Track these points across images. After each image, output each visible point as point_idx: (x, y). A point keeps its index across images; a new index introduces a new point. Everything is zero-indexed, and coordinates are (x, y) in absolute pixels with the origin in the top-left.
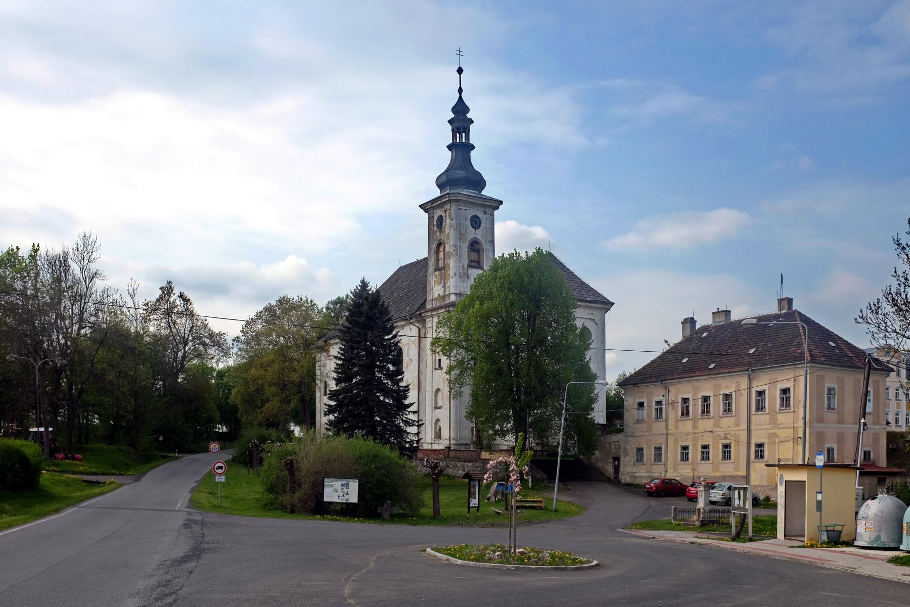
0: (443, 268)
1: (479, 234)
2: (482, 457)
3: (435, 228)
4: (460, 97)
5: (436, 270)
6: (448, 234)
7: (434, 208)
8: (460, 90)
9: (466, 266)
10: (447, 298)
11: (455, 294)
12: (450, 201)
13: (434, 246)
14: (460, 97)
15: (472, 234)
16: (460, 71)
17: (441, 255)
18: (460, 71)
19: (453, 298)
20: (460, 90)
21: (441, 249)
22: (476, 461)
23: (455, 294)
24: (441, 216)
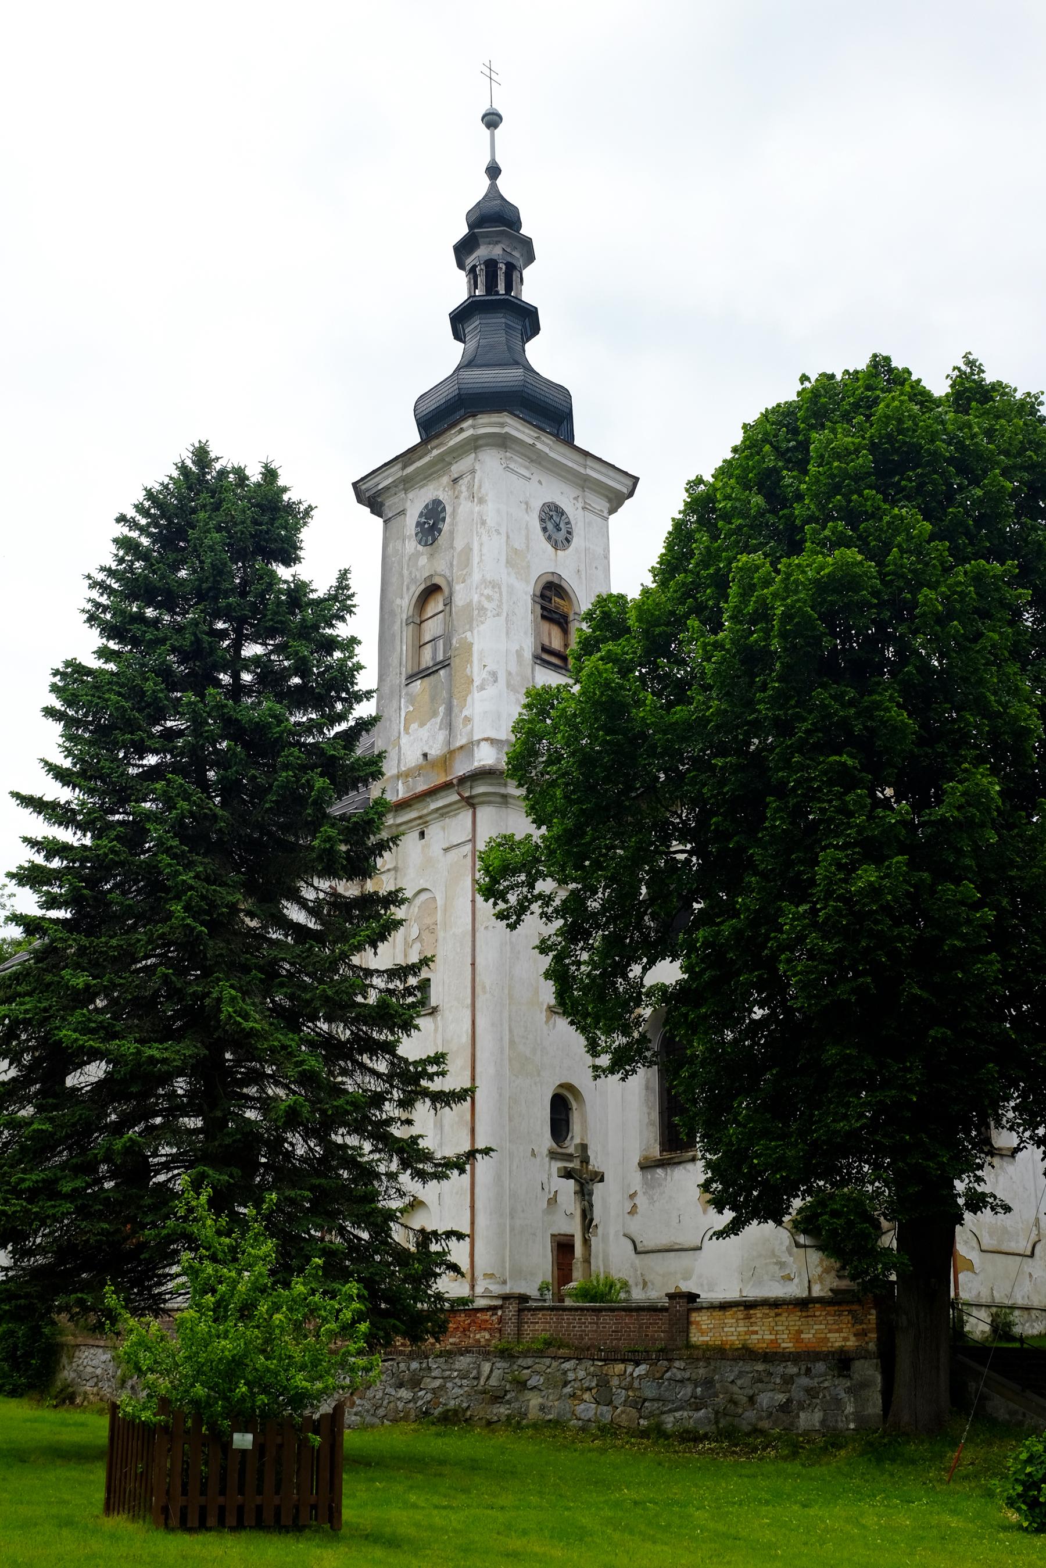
0: (445, 664)
1: (565, 565)
2: (697, 1338)
3: (411, 546)
4: (493, 187)
5: (411, 678)
6: (468, 549)
7: (407, 484)
8: (494, 171)
9: (528, 655)
10: (459, 757)
11: (492, 741)
12: (475, 445)
13: (405, 603)
14: (493, 187)
15: (545, 561)
16: (492, 120)
17: (432, 628)
18: (492, 120)
19: (486, 757)
20: (494, 171)
21: (435, 605)
22: (666, 1354)
23: (492, 741)
24: (437, 503)
